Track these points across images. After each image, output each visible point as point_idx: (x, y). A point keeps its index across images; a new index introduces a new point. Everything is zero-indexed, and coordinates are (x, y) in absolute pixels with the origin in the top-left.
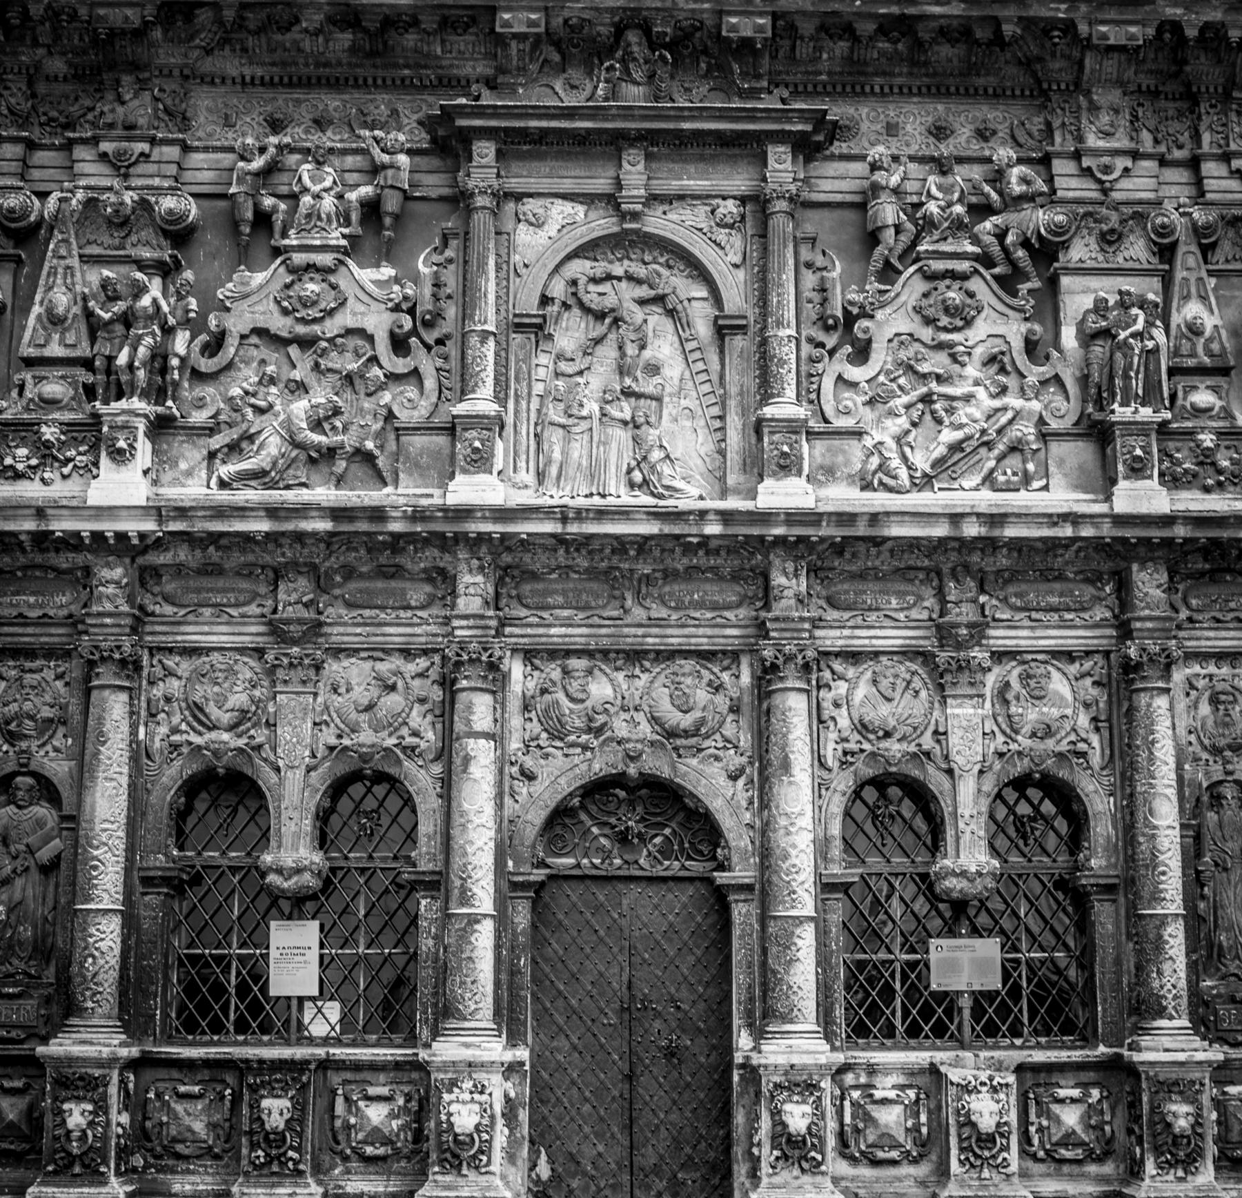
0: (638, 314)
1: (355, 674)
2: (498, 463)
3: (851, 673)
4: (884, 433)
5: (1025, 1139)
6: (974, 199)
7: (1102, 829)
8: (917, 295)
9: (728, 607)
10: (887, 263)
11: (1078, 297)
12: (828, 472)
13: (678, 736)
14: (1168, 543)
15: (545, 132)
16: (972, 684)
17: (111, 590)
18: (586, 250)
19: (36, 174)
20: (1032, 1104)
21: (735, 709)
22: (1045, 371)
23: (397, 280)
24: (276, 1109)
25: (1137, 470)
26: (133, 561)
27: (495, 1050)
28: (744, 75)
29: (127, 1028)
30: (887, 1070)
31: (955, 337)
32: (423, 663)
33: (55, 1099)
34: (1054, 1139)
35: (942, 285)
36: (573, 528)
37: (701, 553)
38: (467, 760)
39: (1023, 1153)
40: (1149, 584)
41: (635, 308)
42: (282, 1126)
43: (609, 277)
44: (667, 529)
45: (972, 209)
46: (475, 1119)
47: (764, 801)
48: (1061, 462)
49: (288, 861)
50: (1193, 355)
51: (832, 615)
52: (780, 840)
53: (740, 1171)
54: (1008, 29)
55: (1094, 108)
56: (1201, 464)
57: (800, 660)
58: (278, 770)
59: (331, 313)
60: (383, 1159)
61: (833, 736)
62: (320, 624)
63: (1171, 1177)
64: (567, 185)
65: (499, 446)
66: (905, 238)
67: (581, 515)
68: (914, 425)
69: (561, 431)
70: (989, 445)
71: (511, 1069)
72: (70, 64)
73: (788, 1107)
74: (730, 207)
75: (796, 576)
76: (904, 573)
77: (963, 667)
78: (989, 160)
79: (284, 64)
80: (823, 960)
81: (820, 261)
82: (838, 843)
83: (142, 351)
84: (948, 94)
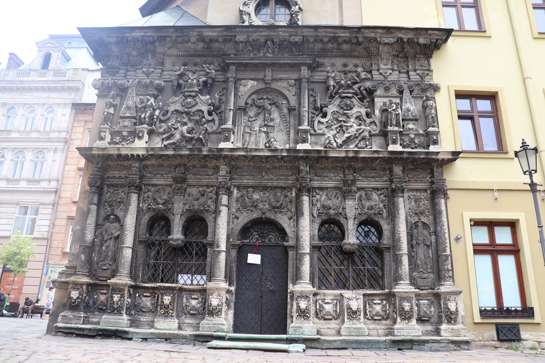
0: (269, 107)
1: (194, 191)
2: (232, 140)
3: (321, 193)
4: (330, 134)
5: (365, 314)
6: (353, 81)
7: (386, 232)
8: (339, 102)
9: (289, 176)
10: (331, 94)
11: (379, 102)
12: (316, 144)
13: (276, 208)
14: (402, 159)
15: (247, 64)
16: (352, 196)
17: (135, 169)
18: (257, 92)
19: (128, 77)
20: (367, 304)
21: (291, 202)
22: (371, 120)
23: (210, 99)
24: (167, 299)
25: (394, 142)
26: (141, 162)
27: (224, 285)
28: (296, 51)
29: (131, 277)
30: (329, 295)
31: (348, 112)
32: (211, 189)
33: (111, 294)
34: (373, 314)
35: (345, 100)
36: (249, 154)
37: (282, 162)
38: (220, 212)
39: (365, 317)
40: (398, 170)
41: (269, 105)
42: (168, 303)
43: (262, 99)
44: (273, 154)
45: (352, 83)
46: (218, 303)
47: (297, 225)
48: (375, 142)
49: (175, 238)
50: (408, 116)
51: (317, 178)
52: (301, 233)
53: (289, 321)
54: (360, 39)
55: (382, 59)
56: (411, 142)
57: (307, 188)
58: (174, 215)
59: (194, 106)
60: (195, 314)
61: (316, 209)
62: (186, 179)
63: (404, 323)
64: (253, 77)
65: (232, 136)
66: (336, 89)
67: (251, 150)
68: (338, 133)
69: (249, 134)
70: (357, 138)
71: (228, 292)
72: (137, 52)
73: (301, 302)
74: (293, 81)
75: (306, 166)
76: (335, 168)
77: (350, 191)
78: (357, 72)
79: (187, 51)
80: (311, 265)
81: (314, 95)
82: (317, 236)
83: (148, 114)
84: (347, 57)
